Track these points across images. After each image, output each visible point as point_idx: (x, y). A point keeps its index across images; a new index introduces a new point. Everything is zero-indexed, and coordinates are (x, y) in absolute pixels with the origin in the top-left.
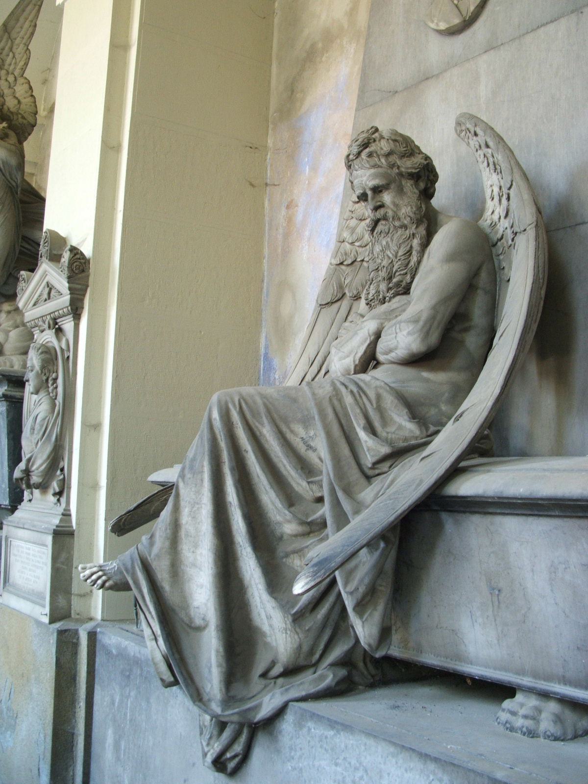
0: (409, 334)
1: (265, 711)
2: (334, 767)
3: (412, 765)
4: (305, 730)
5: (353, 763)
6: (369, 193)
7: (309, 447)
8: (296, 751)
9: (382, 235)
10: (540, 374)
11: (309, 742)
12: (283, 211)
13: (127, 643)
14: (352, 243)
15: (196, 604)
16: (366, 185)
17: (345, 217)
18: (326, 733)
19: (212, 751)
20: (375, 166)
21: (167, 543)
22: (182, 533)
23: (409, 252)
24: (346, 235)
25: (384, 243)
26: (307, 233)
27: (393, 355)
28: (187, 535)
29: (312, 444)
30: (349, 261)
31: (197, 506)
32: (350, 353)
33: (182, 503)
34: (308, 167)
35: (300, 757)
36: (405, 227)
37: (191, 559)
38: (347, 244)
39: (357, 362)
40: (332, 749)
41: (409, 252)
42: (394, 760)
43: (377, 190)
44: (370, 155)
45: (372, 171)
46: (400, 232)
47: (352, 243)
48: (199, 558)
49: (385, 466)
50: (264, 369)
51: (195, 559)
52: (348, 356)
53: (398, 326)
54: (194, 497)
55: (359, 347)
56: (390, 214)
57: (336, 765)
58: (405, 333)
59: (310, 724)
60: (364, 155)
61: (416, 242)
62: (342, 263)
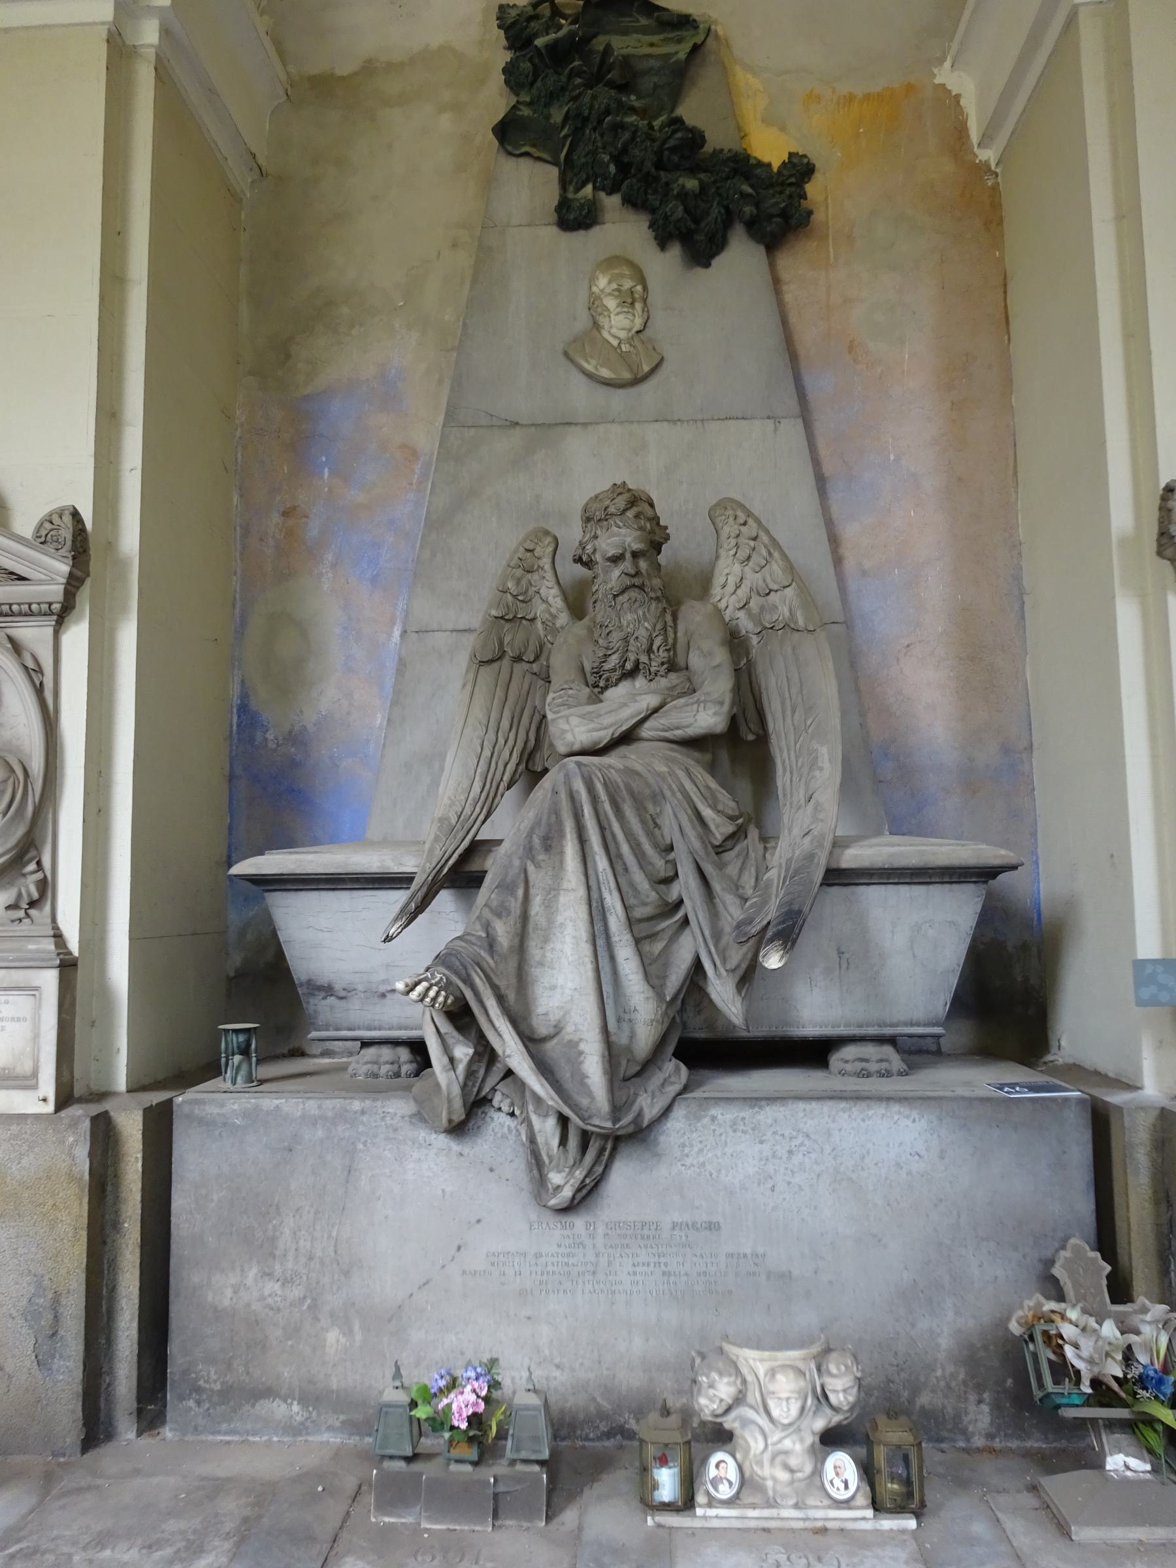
0: (715, 714)
1: (649, 1114)
2: (758, 1147)
3: (871, 1112)
4: (706, 1120)
5: (787, 1133)
6: (628, 555)
7: (656, 825)
8: (692, 1146)
9: (637, 604)
10: (734, 761)
11: (714, 1131)
12: (276, 518)
13: (277, 1102)
14: (515, 596)
15: (541, 1010)
16: (629, 546)
17: (512, 564)
18: (742, 1114)
19: (572, 1181)
20: (641, 529)
21: (517, 940)
22: (531, 927)
23: (665, 629)
24: (510, 585)
25: (640, 612)
26: (329, 557)
27: (679, 733)
28: (536, 929)
29: (658, 822)
30: (510, 616)
31: (553, 893)
32: (611, 725)
33: (532, 891)
34: (326, 470)
35: (701, 1150)
36: (657, 599)
37: (537, 958)
38: (509, 596)
39: (616, 735)
40: (753, 1129)
41: (665, 629)
42: (846, 1115)
43: (635, 555)
44: (637, 516)
45: (639, 533)
46: (654, 604)
47: (515, 596)
48: (549, 954)
49: (729, 844)
50: (239, 725)
51: (544, 956)
52: (605, 728)
53: (702, 705)
54: (550, 882)
55: (627, 720)
56: (647, 582)
57: (761, 1142)
58: (710, 712)
59: (715, 1111)
60: (630, 514)
61: (668, 618)
62: (502, 618)
